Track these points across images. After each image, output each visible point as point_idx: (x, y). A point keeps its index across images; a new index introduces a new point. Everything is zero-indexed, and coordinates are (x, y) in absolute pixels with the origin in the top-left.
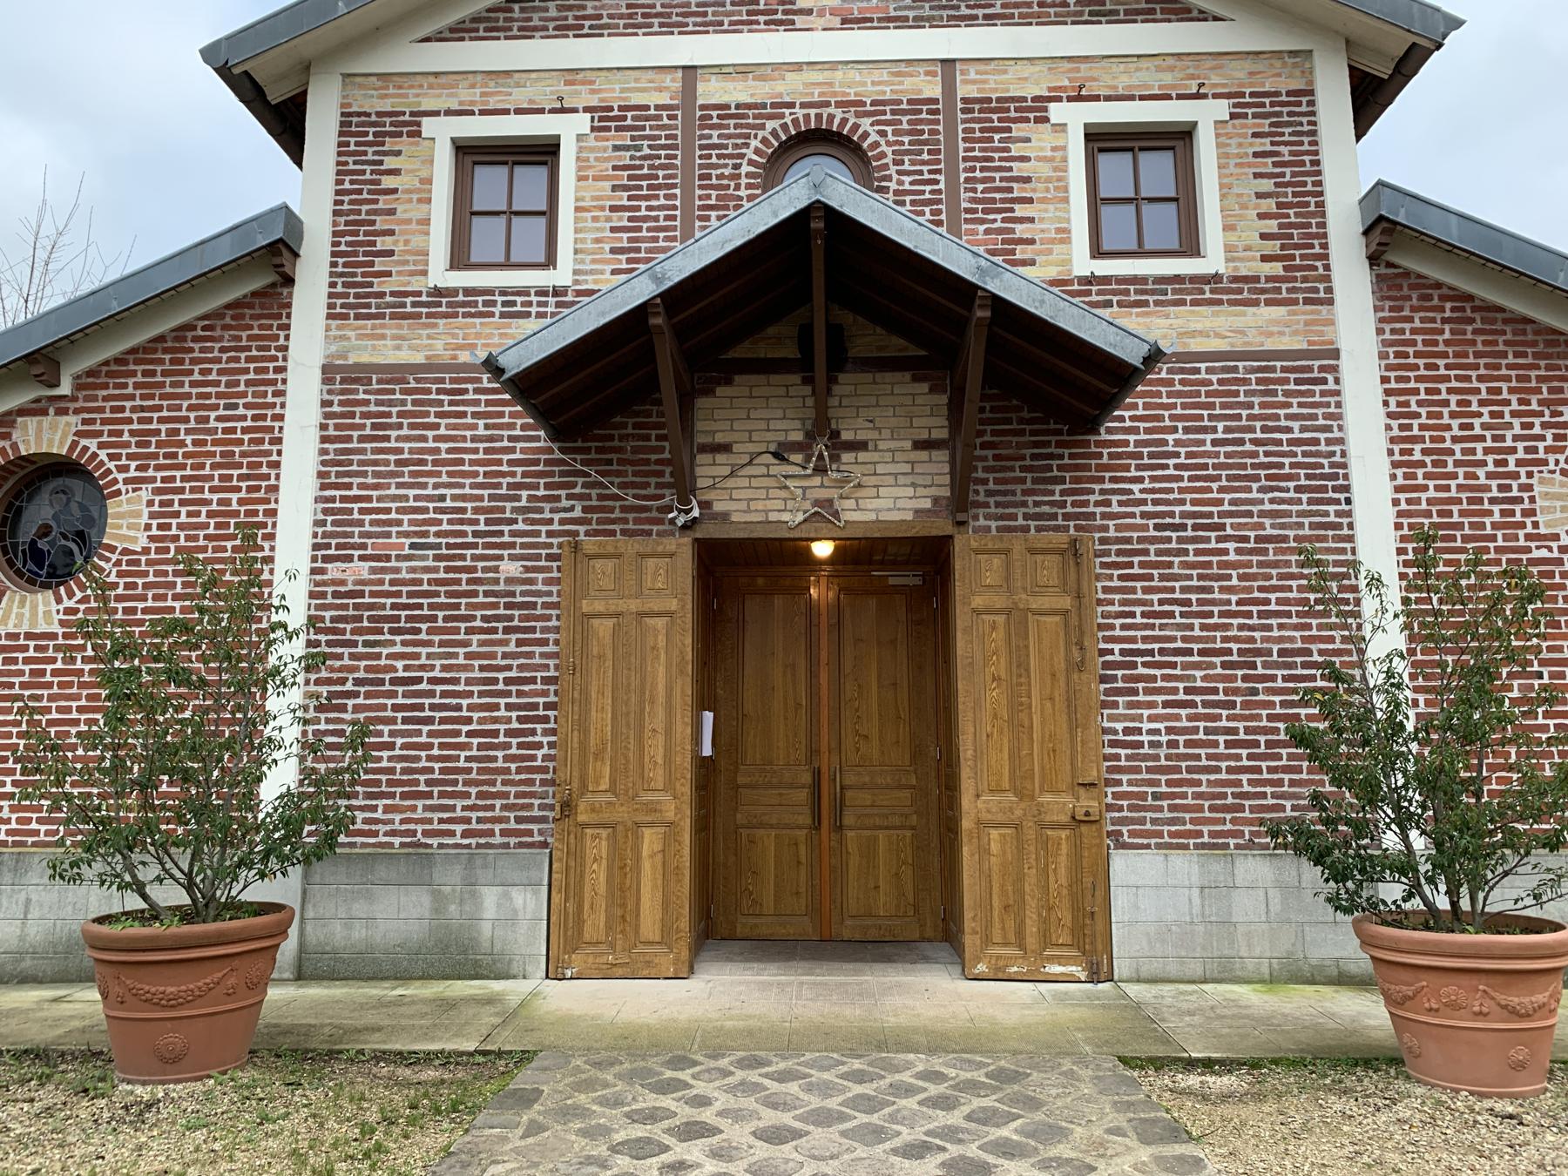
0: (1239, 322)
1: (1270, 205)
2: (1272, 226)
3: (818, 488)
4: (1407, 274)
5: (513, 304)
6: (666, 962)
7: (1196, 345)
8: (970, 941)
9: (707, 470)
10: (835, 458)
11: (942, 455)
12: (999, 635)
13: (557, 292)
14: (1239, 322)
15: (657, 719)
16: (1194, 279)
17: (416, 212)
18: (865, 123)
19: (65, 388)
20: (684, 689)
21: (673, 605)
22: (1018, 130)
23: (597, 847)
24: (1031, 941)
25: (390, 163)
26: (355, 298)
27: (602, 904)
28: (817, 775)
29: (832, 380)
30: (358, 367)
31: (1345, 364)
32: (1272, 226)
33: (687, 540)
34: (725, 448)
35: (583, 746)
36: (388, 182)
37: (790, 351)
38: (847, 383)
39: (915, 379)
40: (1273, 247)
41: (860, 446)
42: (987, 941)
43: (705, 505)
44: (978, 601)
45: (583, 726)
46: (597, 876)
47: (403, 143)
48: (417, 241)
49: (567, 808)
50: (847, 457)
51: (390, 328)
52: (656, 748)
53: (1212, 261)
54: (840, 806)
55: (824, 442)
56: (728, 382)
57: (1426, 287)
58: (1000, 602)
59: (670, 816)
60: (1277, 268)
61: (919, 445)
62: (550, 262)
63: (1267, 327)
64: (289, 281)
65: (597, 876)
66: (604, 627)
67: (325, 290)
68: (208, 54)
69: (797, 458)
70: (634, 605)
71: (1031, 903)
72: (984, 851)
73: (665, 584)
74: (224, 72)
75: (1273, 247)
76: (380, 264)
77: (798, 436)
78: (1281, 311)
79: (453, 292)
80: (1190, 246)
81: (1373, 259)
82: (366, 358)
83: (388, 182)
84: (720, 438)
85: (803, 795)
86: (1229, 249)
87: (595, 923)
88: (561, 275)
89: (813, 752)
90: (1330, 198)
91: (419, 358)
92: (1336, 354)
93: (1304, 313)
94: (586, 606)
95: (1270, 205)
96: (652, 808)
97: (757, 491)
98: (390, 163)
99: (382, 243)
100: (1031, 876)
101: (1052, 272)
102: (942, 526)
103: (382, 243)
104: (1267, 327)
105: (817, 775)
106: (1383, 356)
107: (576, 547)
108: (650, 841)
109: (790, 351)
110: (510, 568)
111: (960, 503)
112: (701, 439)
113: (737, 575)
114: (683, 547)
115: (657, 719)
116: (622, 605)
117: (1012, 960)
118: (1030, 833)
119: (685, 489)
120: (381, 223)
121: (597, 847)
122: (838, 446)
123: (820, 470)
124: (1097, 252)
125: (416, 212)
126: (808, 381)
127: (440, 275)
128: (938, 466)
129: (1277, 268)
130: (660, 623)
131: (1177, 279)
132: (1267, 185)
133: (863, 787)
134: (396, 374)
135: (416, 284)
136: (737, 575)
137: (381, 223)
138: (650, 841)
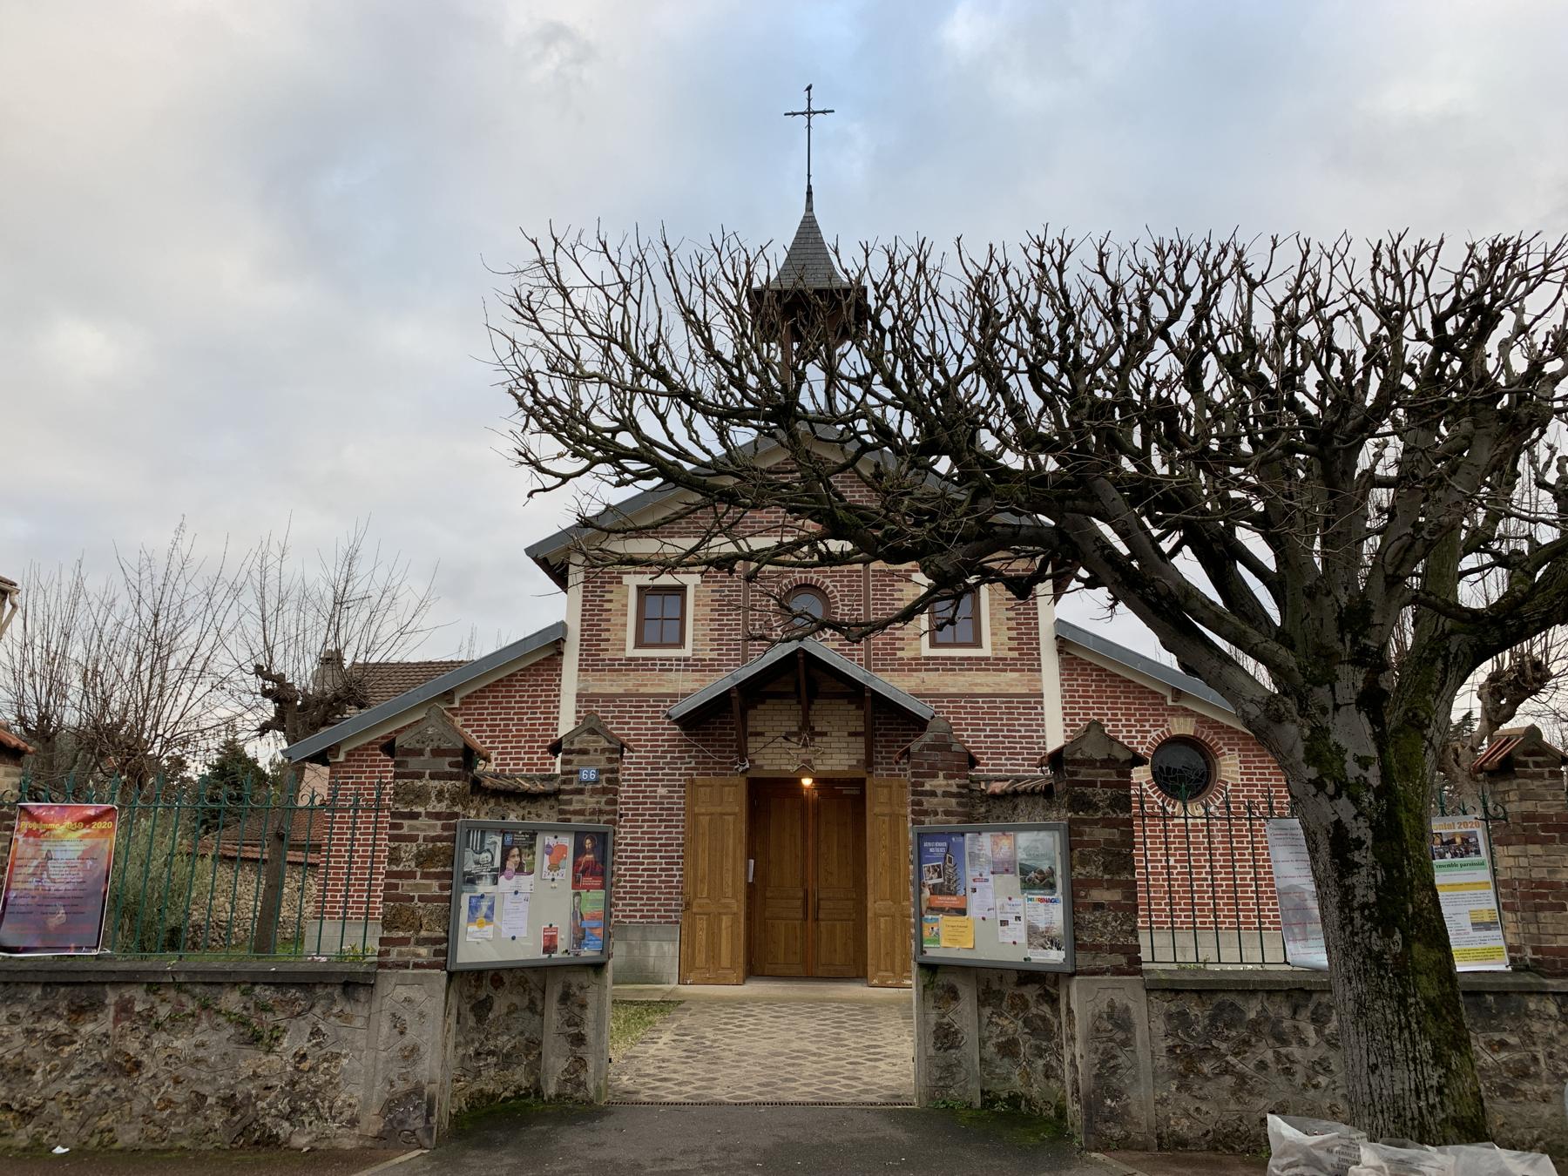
0: (997, 679)
1: (1013, 624)
2: (1013, 634)
3: (805, 754)
4: (1076, 658)
5: (665, 666)
6: (733, 977)
7: (978, 690)
8: (870, 970)
9: (753, 745)
10: (812, 740)
11: (861, 739)
12: (886, 826)
13: (686, 659)
14: (997, 679)
15: (729, 864)
16: (977, 658)
17: (620, 620)
18: (827, 581)
19: (457, 705)
20: (742, 851)
21: (737, 809)
22: (898, 585)
23: (702, 924)
24: (898, 969)
25: (608, 596)
26: (591, 662)
27: (703, 950)
28: (806, 892)
29: (810, 703)
30: (592, 695)
31: (1046, 700)
32: (1013, 634)
33: (743, 779)
34: (762, 734)
35: (695, 876)
36: (607, 606)
37: (791, 689)
38: (818, 704)
39: (850, 703)
40: (1014, 644)
41: (824, 734)
42: (878, 969)
43: (751, 761)
44: (877, 810)
45: (695, 866)
46: (702, 936)
47: (614, 587)
48: (620, 634)
49: (688, 905)
50: (818, 739)
51: (608, 676)
52: (728, 878)
53: (986, 651)
54: (818, 909)
55: (807, 732)
56: (763, 702)
57: (1082, 662)
58: (887, 810)
59: (735, 909)
60: (1015, 654)
61: (851, 734)
62: (681, 644)
63: (1010, 682)
64: (561, 654)
65: (702, 936)
66: (705, 820)
67: (577, 657)
68: (529, 551)
69: (795, 739)
70: (719, 809)
71: (898, 951)
72: (878, 928)
73: (734, 801)
74: (536, 560)
75: (1014, 644)
76: (603, 645)
77: (795, 729)
78: (1015, 675)
79: (637, 659)
80: (977, 643)
81: (1060, 651)
82: (596, 691)
83: (607, 606)
84: (759, 730)
85: (799, 903)
86: (993, 644)
87: (701, 959)
88: (687, 652)
89: (804, 881)
90: (1040, 621)
91: (621, 691)
92: (1042, 696)
93: (1027, 676)
94: (696, 810)
95: (1013, 624)
96: (727, 906)
97: (775, 755)
98: (608, 596)
99: (604, 635)
100: (898, 938)
101: (912, 654)
102: (861, 773)
103: (604, 635)
104: (1010, 682)
105: (806, 892)
106: (1063, 697)
107: (692, 781)
108: (726, 921)
109: (791, 689)
110: (662, 791)
111: (869, 763)
112: (750, 730)
113: (768, 796)
114: (741, 782)
115: (729, 864)
116: (713, 810)
117: (888, 978)
118: (898, 920)
119: (743, 754)
120: (604, 625)
121: (702, 924)
122: (814, 734)
123: (805, 745)
124: (933, 644)
125: (620, 620)
126: (799, 703)
127: (631, 651)
128: (859, 744)
129: (1015, 654)
130: (731, 818)
131: (969, 658)
132: (1012, 614)
133: (829, 899)
134: (610, 698)
135: (620, 655)
136: (768, 796)
137: (604, 625)
138: (726, 921)
